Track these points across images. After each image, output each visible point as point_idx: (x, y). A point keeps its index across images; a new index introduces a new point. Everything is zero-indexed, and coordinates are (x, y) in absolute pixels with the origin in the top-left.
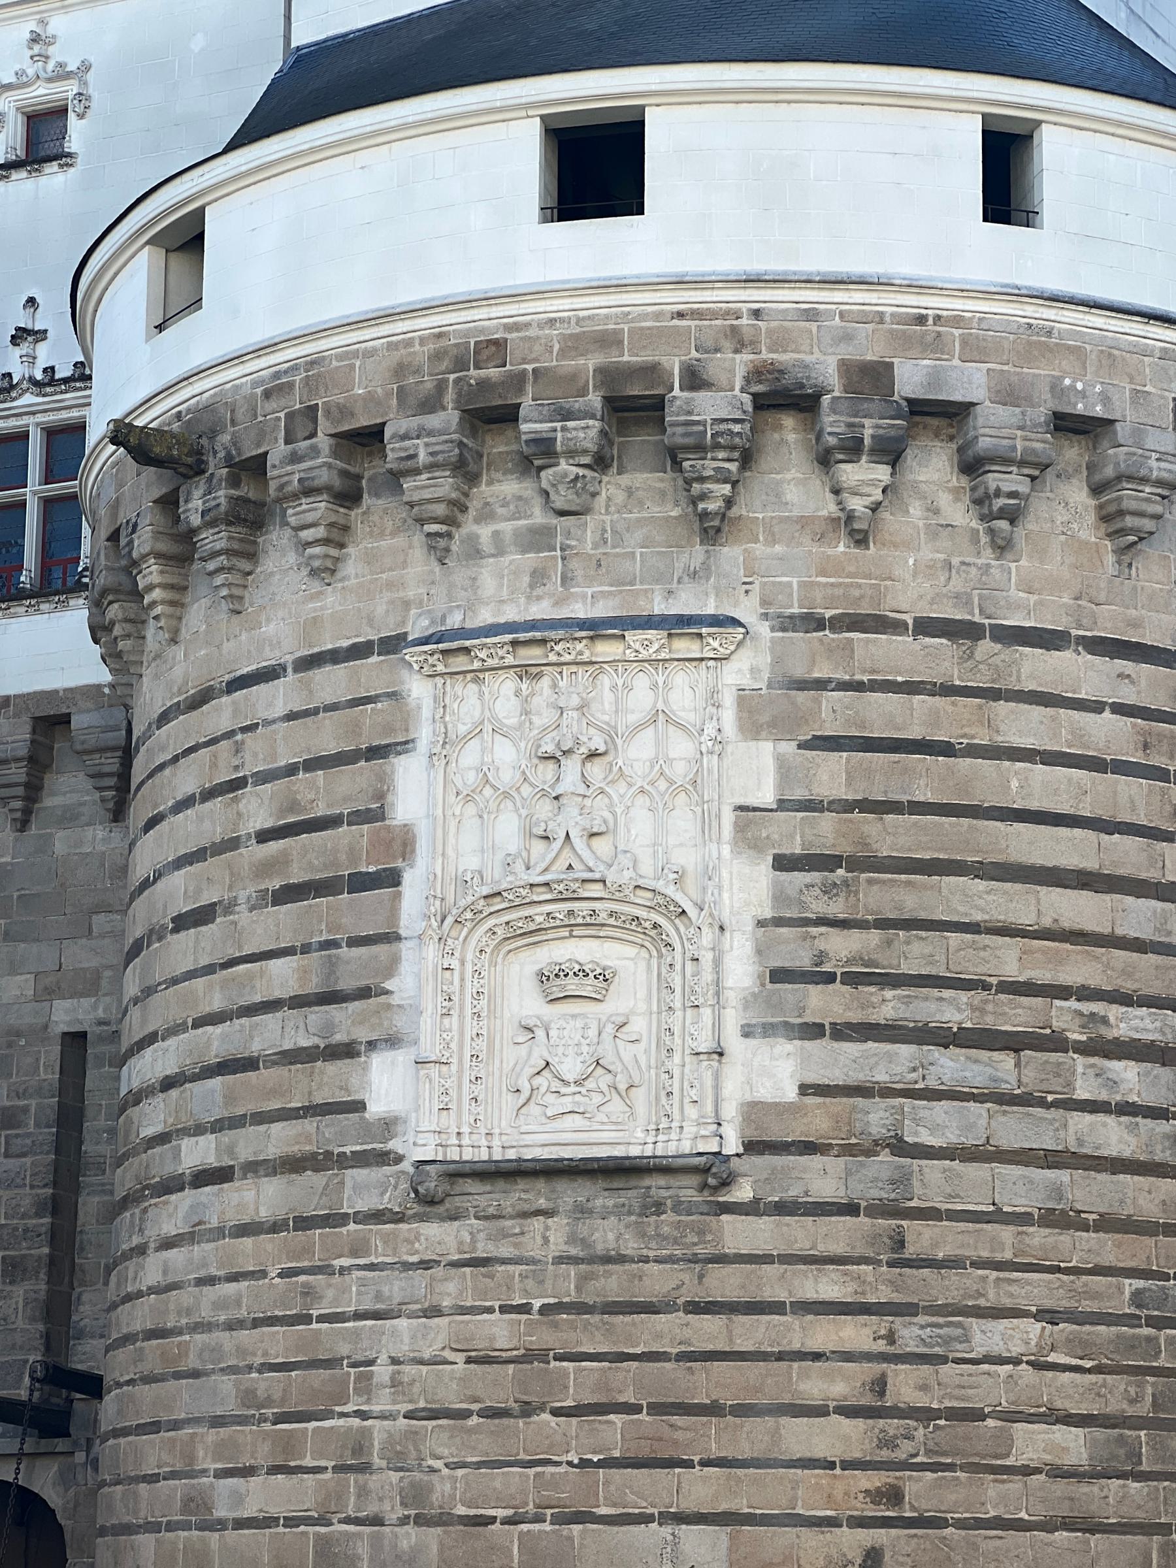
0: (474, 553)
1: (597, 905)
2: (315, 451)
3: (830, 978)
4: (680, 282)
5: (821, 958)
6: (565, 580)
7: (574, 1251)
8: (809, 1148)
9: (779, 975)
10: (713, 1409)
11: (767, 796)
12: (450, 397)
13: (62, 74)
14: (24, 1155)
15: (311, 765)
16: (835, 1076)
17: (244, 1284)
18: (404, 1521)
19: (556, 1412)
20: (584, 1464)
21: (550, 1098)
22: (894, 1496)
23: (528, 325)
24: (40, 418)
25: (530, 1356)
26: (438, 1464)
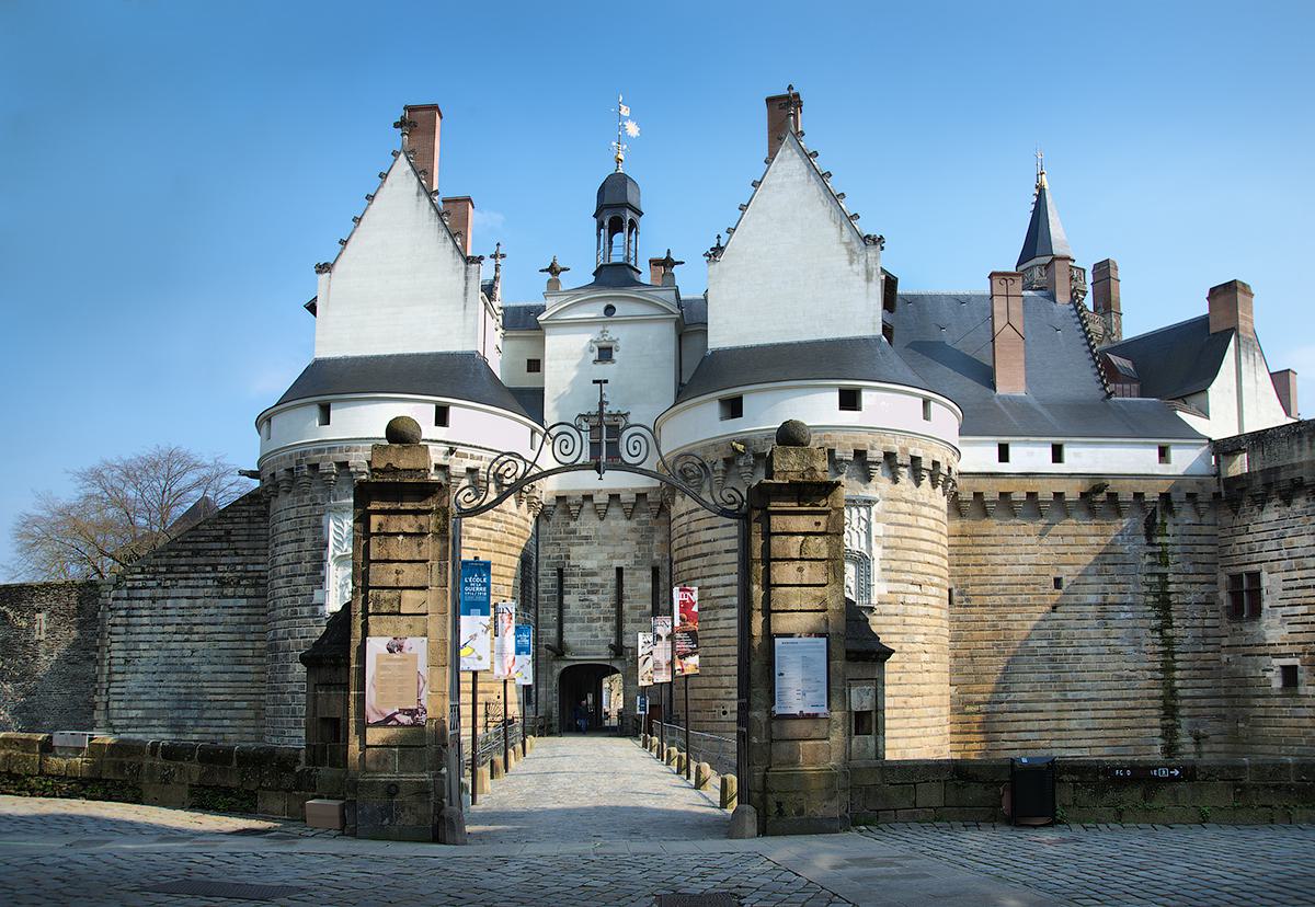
9: (883, 570)
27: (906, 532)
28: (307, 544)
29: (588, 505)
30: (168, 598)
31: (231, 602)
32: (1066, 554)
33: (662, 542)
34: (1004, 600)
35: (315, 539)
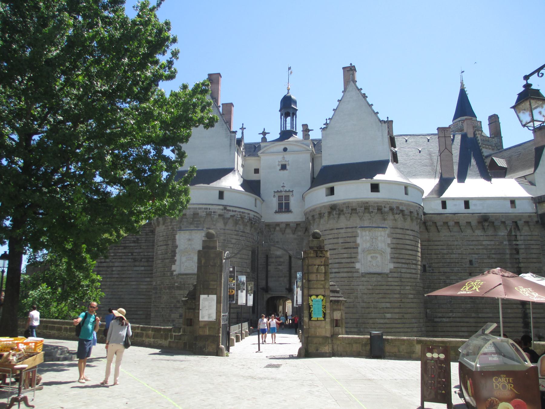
0: (364, 220)
8: (394, 272)
10: (388, 294)
11: (390, 242)
13: (286, 161)
15: (347, 237)
16: (396, 266)
22: (401, 300)
27: (401, 242)
28: (170, 247)
29: (278, 228)
31: (137, 268)
32: (473, 249)
34: (447, 270)
35: (173, 244)
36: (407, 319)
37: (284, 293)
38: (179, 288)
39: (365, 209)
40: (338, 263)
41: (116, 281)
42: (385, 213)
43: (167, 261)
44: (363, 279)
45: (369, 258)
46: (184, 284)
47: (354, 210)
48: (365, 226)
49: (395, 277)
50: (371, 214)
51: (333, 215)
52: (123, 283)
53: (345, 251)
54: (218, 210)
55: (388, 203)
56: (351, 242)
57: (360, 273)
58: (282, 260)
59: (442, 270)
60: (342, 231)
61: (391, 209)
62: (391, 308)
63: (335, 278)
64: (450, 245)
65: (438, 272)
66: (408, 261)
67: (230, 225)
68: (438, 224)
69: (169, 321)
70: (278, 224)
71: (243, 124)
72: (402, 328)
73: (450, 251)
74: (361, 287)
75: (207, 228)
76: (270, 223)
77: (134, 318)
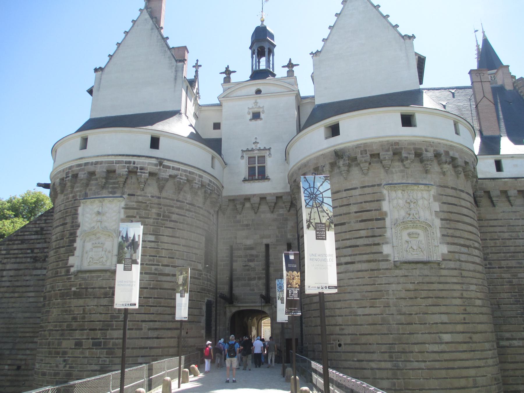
0: (392, 173)
1: (417, 224)
2: (367, 156)
3: (449, 236)
4: (424, 137)
5: (448, 233)
6: (407, 177)
7: (421, 274)
8: (450, 260)
9: (443, 235)
10: (443, 298)
11: (438, 210)
12: (391, 150)
14: (260, 261)
15: (365, 202)
16: (452, 250)
17: (360, 279)
18: (398, 314)
19: (421, 298)
20: (426, 306)
21: (412, 252)
22: (465, 310)
23: (402, 141)
24: (258, 155)
25: (415, 290)
26: (402, 306)
29: (248, 205)
30: (4, 270)
33: (292, 227)
34: (513, 263)
35: (73, 222)
36: (476, 343)
37: (257, 305)
38: (77, 295)
39: (394, 154)
40: (350, 247)
41: (6, 292)
42: (428, 160)
43: (62, 250)
44: (397, 272)
45: (405, 237)
46: (86, 288)
47: (375, 156)
48: (395, 182)
49: (452, 269)
50: (405, 163)
51: (339, 167)
52: (16, 295)
53: (363, 225)
54: (150, 165)
55: (431, 144)
56: (372, 210)
57: (392, 262)
58: (254, 252)
59: (503, 263)
60: (357, 192)
61: (437, 155)
62: (450, 323)
63: (346, 272)
64: (513, 226)
65: (499, 268)
66: (468, 243)
67: (169, 191)
68: (493, 194)
69: (58, 353)
70: (247, 199)
71: (197, 61)
72: (471, 359)
73: (514, 234)
74: (394, 287)
75: (129, 195)
76: (235, 196)
77: (28, 349)
